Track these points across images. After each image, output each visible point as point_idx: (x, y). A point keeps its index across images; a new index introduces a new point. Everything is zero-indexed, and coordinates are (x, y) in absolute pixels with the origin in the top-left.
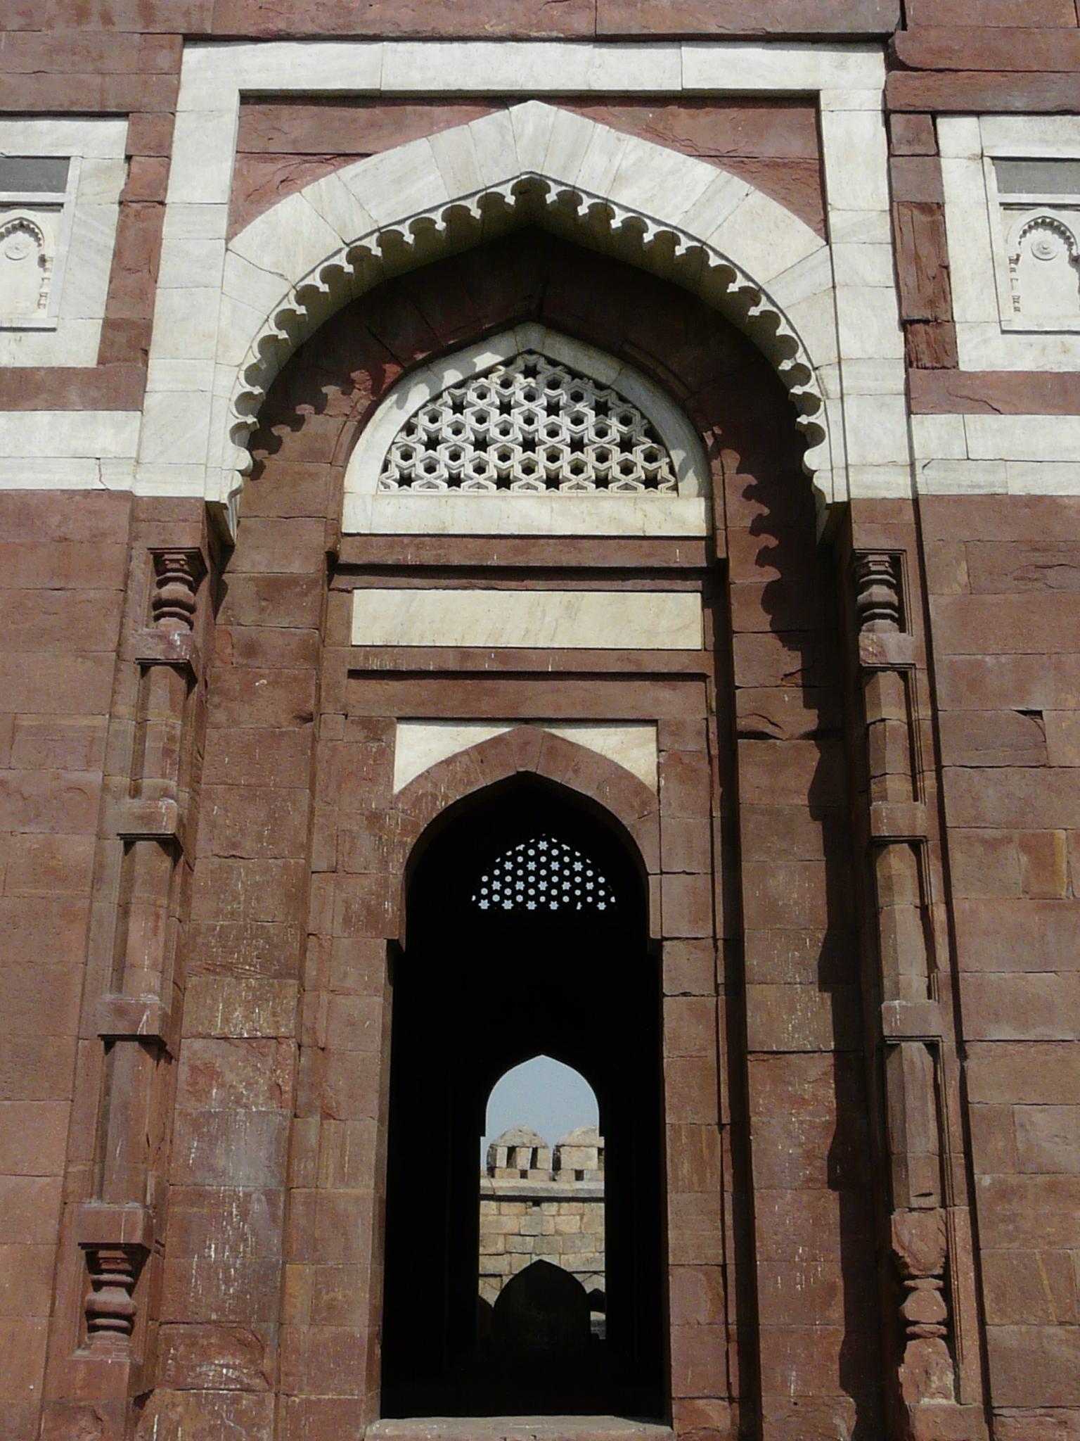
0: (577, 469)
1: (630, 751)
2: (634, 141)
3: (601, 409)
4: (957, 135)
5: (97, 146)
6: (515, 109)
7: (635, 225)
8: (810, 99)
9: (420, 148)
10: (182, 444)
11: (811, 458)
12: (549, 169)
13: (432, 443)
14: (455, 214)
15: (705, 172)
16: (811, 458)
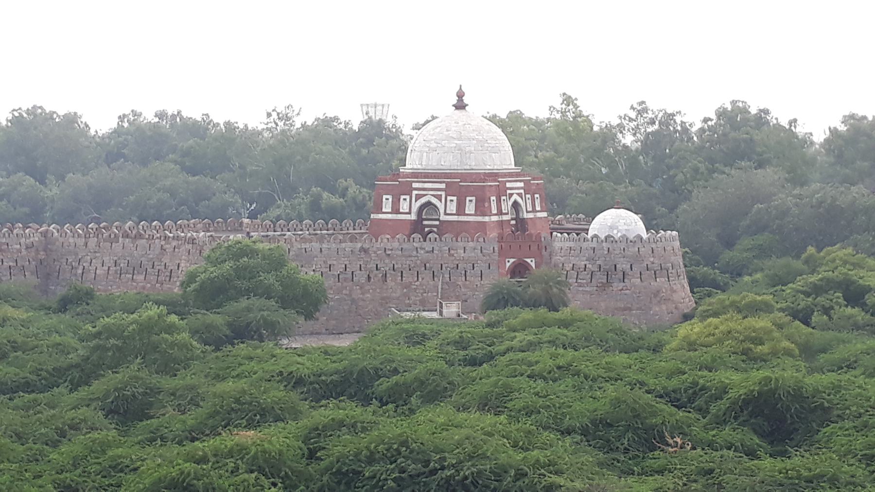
5: (408, 197)
10: (413, 217)
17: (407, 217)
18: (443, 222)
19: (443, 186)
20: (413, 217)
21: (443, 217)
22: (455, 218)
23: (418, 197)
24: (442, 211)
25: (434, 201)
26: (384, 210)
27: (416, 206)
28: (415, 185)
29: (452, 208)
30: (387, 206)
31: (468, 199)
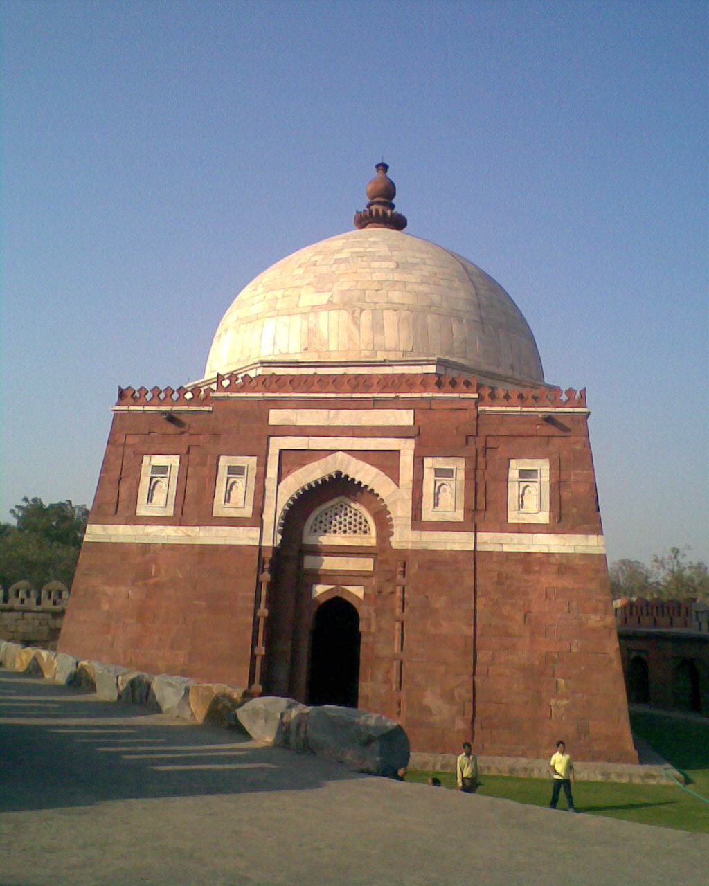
0: (350, 529)
1: (357, 591)
2: (361, 462)
3: (356, 515)
4: (428, 462)
5: (251, 462)
6: (337, 453)
7: (360, 483)
8: (398, 451)
9: (316, 463)
11: (391, 539)
12: (342, 470)
13: (321, 522)
14: (323, 480)
15: (374, 470)
16: (391, 539)
17: (246, 537)
18: (404, 558)
19: (405, 418)
20: (271, 538)
21: (403, 537)
22: (459, 542)
23: (290, 460)
24: (400, 511)
25: (364, 473)
26: (142, 511)
27: (281, 495)
28: (276, 417)
29: (448, 502)
30: (159, 498)
31: (516, 466)
